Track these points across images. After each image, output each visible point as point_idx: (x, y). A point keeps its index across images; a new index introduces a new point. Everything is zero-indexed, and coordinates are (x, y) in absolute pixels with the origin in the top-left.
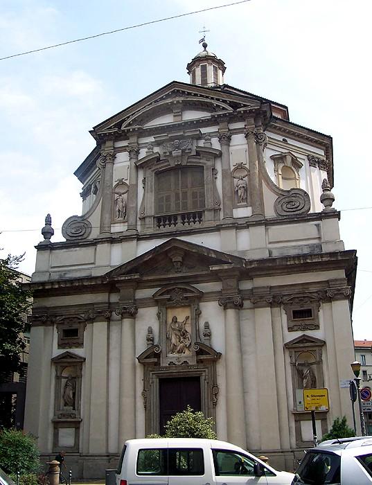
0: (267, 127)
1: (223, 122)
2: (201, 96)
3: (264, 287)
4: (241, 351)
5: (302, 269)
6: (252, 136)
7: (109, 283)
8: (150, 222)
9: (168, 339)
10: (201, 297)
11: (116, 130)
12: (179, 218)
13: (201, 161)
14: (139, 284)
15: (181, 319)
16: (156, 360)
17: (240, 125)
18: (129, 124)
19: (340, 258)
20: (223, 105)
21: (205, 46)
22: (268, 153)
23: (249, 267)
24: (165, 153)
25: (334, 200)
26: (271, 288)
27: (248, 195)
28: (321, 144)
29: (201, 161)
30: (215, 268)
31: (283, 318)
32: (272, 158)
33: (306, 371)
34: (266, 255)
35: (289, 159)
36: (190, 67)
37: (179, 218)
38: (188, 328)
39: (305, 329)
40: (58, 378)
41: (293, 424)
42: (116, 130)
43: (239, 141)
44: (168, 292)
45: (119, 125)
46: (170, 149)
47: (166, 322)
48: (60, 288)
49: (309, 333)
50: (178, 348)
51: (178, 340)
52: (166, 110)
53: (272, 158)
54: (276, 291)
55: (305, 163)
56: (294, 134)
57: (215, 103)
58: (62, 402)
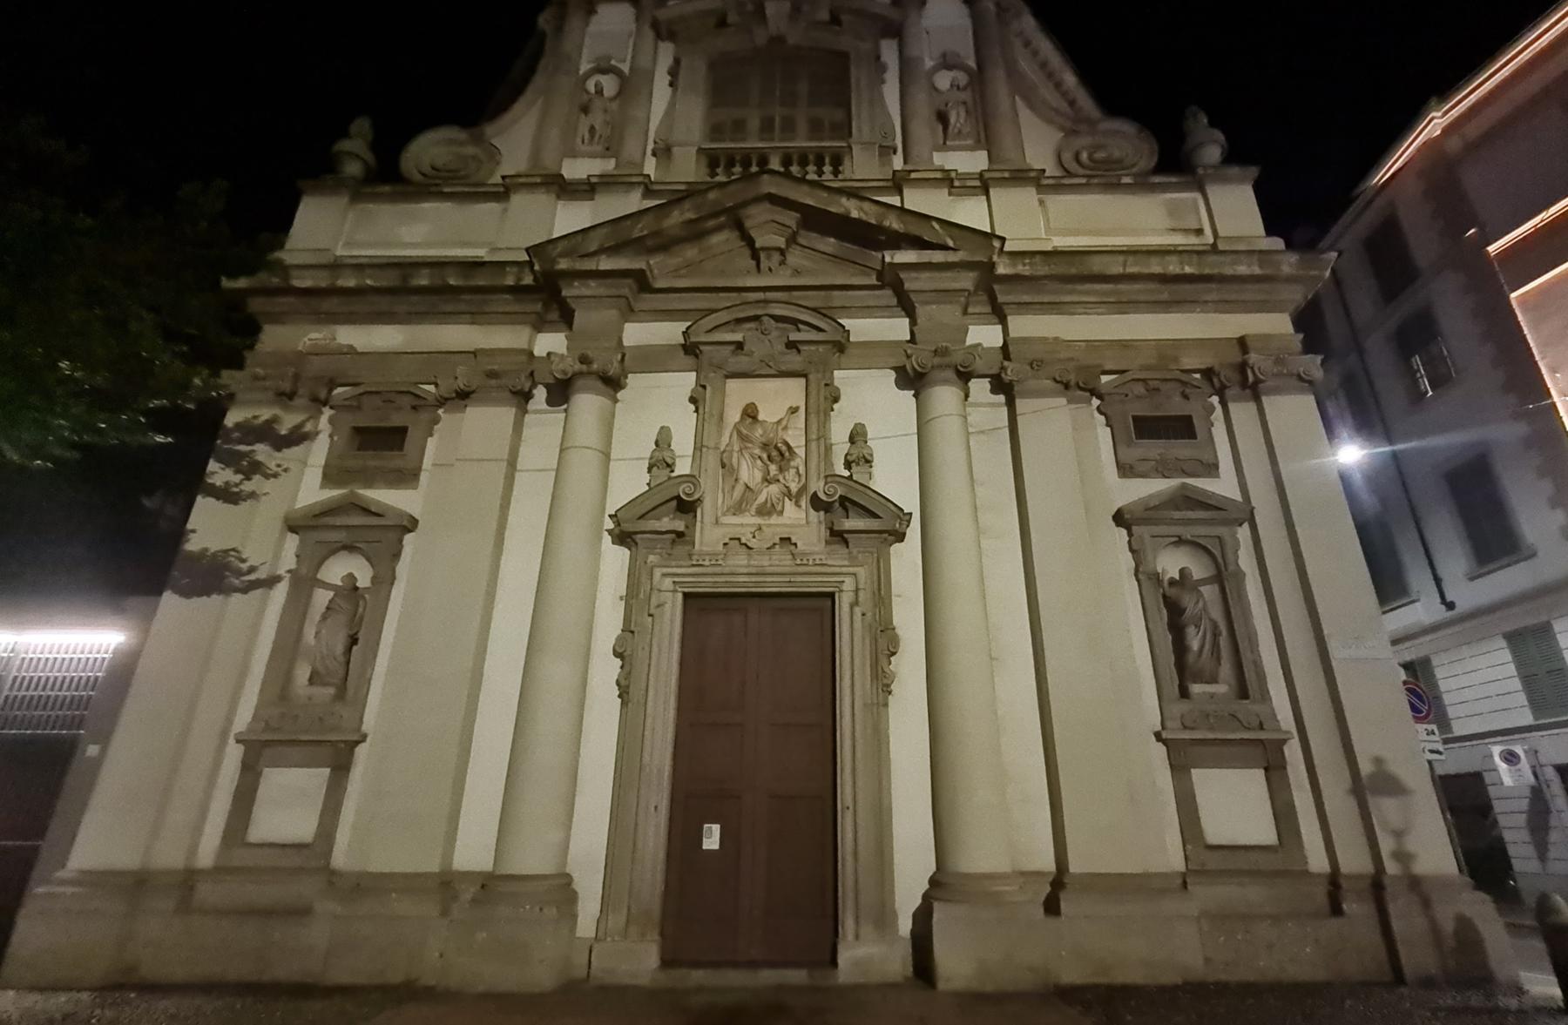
7: (544, 288)
16: (679, 525)
38: (795, 437)
47: (721, 418)
50: (761, 499)
51: (758, 475)
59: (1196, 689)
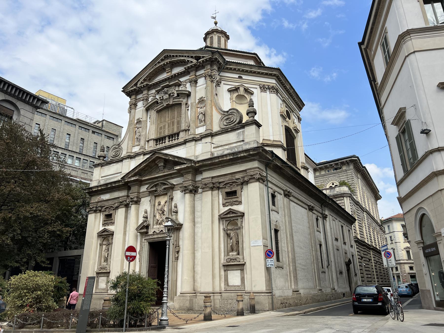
0: (221, 69)
1: (192, 71)
2: (180, 56)
3: (208, 178)
4: (194, 222)
5: (230, 163)
6: (208, 77)
8: (152, 143)
9: (155, 216)
10: (172, 188)
11: (135, 87)
12: (167, 138)
13: (180, 100)
14: (140, 183)
15: (163, 203)
17: (202, 72)
18: (142, 83)
19: (251, 153)
20: (190, 59)
21: (216, 23)
22: (224, 87)
23: (197, 165)
24: (160, 98)
25: (256, 114)
26: (213, 178)
27: (203, 118)
28: (271, 75)
29: (180, 100)
30: (178, 168)
31: (219, 197)
32: (230, 91)
33: (232, 234)
34: (208, 156)
35: (242, 89)
36: (205, 39)
37: (167, 138)
39: (232, 205)
40: (101, 245)
41: (223, 273)
42: (135, 87)
43: (201, 81)
44: (156, 186)
45: (136, 85)
46: (163, 95)
48: (98, 190)
49: (235, 208)
50: (159, 222)
52: (162, 70)
53: (230, 91)
54: (215, 181)
55: (256, 91)
56: (247, 71)
57: (187, 59)
58: (103, 260)
59: (230, 254)
